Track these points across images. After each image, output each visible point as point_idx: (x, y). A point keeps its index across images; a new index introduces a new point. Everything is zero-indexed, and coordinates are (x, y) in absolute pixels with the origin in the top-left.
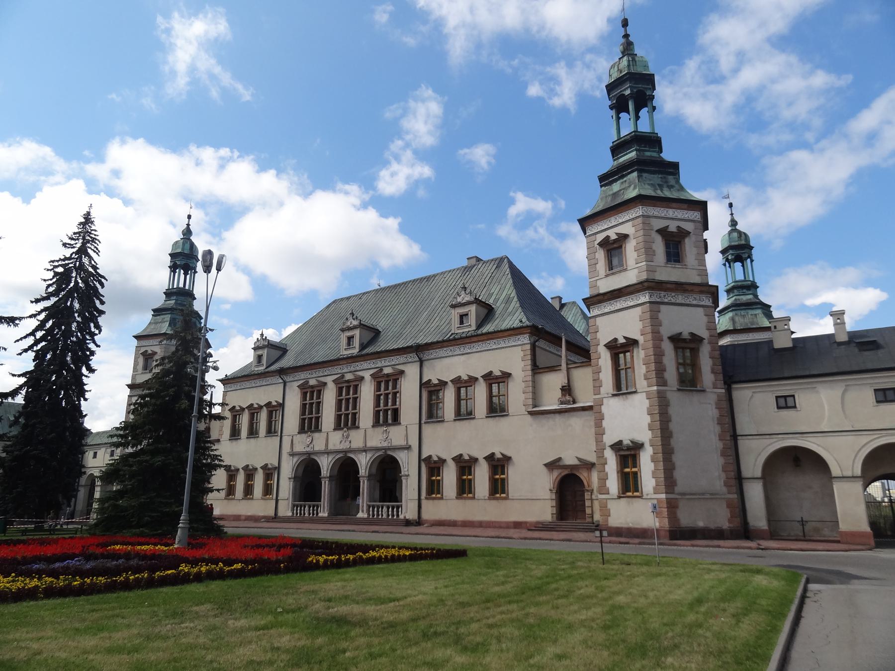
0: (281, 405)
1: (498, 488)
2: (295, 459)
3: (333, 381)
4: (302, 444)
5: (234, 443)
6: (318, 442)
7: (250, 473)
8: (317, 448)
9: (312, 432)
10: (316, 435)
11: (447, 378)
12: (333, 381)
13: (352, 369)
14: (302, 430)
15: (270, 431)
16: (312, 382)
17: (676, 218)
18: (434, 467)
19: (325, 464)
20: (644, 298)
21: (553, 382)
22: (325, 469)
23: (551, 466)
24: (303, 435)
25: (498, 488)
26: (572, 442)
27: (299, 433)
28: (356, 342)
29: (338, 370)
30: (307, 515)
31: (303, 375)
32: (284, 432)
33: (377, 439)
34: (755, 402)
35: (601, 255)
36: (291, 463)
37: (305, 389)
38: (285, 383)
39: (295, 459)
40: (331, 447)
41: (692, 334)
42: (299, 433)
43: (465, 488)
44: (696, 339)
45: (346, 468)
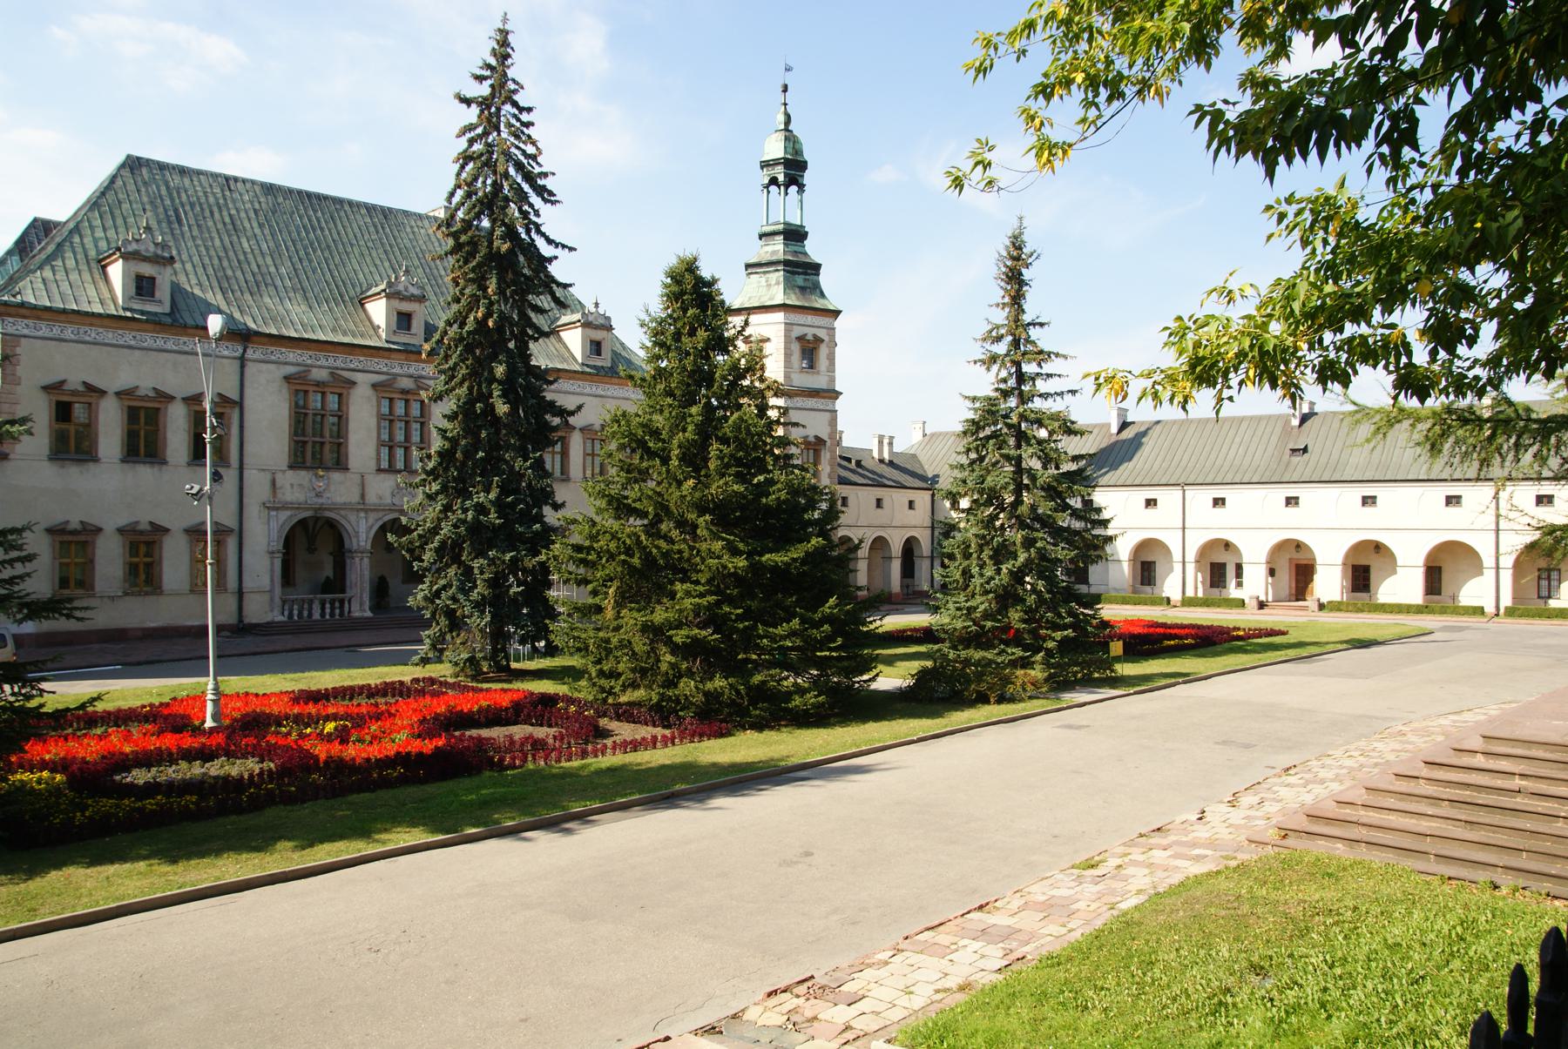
0: (240, 404)
2: (284, 515)
3: (374, 386)
4: (298, 488)
5: (73, 471)
6: (339, 490)
8: (339, 499)
9: (327, 469)
10: (336, 476)
12: (374, 386)
13: (412, 371)
14: (297, 463)
16: (320, 374)
17: (810, 325)
19: (361, 532)
22: (363, 536)
24: (303, 473)
27: (291, 467)
29: (381, 364)
30: (317, 616)
31: (292, 355)
32: (246, 460)
35: (796, 347)
36: (274, 525)
38: (243, 361)
39: (284, 515)
40: (371, 498)
41: (817, 437)
42: (291, 467)
44: (820, 441)
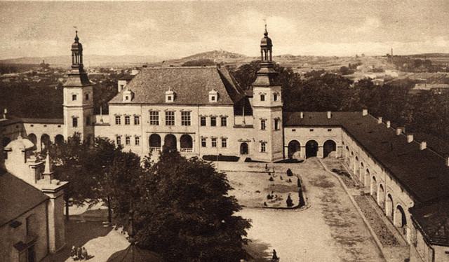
1: (224, 145)
7: (128, 138)
11: (208, 115)
15: (136, 123)
18: (203, 139)
20: (270, 110)
21: (239, 120)
23: (240, 141)
25: (224, 145)
26: (244, 135)
28: (172, 99)
33: (183, 129)
34: (288, 131)
37: (151, 112)
43: (214, 145)
45: (170, 137)
